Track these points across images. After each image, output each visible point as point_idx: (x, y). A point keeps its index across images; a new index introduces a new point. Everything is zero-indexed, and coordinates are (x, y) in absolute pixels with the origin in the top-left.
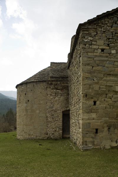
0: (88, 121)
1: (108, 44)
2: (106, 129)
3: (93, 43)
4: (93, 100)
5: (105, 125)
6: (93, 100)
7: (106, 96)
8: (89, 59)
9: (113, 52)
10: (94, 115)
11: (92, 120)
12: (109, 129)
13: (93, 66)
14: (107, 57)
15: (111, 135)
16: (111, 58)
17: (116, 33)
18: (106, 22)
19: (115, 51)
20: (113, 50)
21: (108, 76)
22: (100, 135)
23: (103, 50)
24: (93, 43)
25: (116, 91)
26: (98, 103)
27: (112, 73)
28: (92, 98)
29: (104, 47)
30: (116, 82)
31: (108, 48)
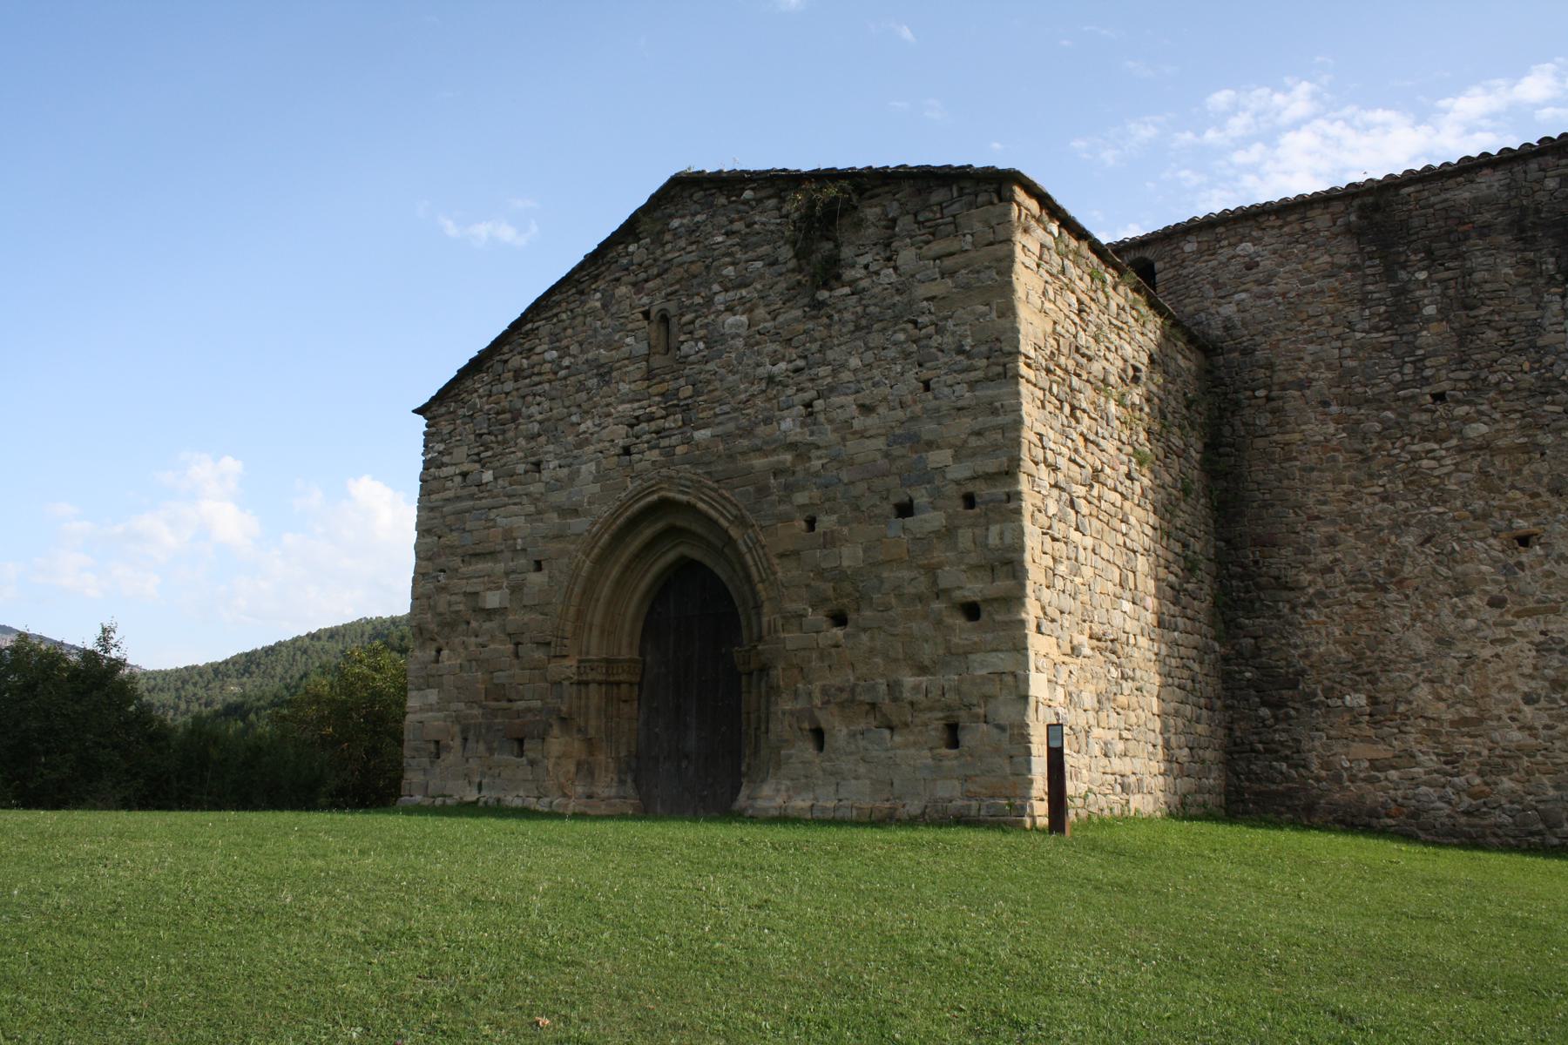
0: (418, 717)
1: (478, 454)
2: (457, 742)
3: (446, 459)
4: (434, 646)
5: (457, 728)
6: (434, 646)
7: (465, 627)
8: (431, 514)
9: (488, 476)
10: (433, 696)
11: (428, 711)
12: (465, 739)
13: (439, 533)
14: (472, 497)
15: (467, 760)
16: (480, 499)
17: (498, 413)
18: (477, 385)
19: (491, 472)
20: (488, 469)
21: (473, 560)
22: (449, 759)
23: (464, 475)
24: (446, 459)
25: (484, 610)
26: (445, 653)
27: (479, 549)
28: (433, 640)
29: (466, 467)
30: (489, 576)
31: (478, 466)
